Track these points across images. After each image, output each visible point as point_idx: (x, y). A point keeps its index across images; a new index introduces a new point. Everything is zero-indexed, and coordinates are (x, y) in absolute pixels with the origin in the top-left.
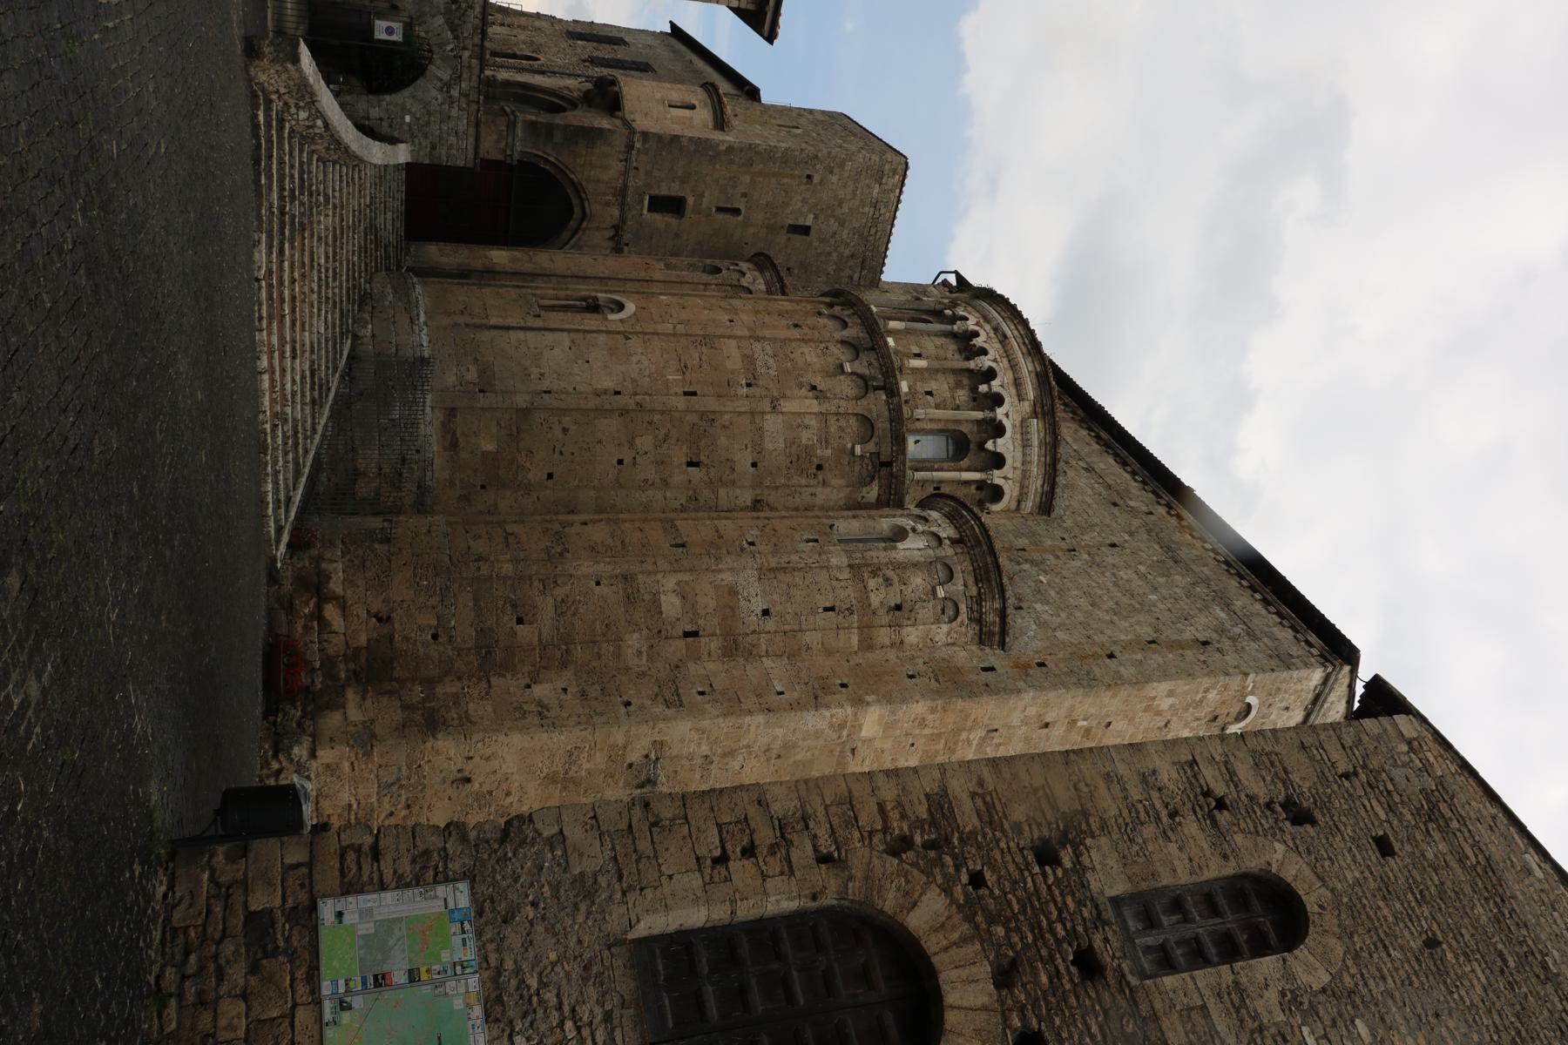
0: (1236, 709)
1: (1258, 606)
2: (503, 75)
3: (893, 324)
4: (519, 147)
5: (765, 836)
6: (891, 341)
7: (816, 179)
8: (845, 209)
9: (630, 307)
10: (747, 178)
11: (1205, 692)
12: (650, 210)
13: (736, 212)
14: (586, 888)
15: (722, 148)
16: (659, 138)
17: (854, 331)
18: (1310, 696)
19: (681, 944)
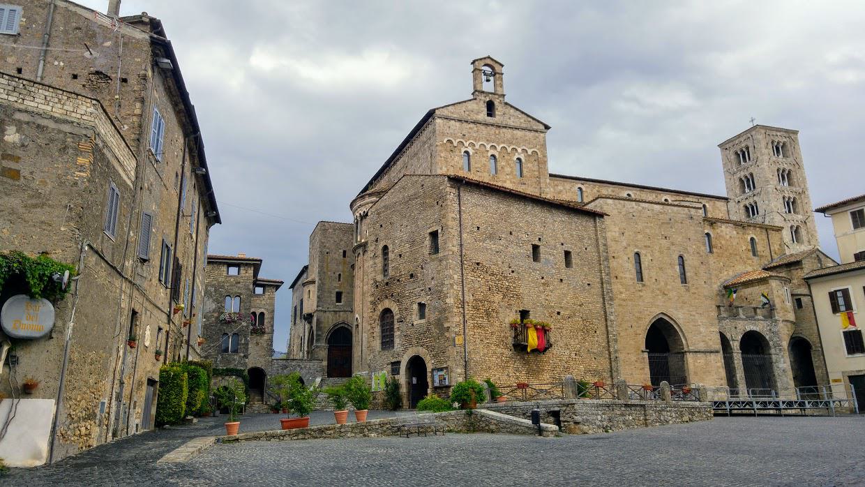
0: (449, 144)
1: (426, 132)
2: (306, 349)
3: (359, 240)
4: (324, 345)
5: (372, 331)
6: (363, 241)
7: (328, 250)
8: (336, 240)
9: (357, 316)
10: (329, 273)
11: (441, 157)
12: (340, 302)
13: (340, 275)
14: (374, 356)
15: (320, 282)
16: (318, 302)
17: (360, 251)
18: (445, 120)
19: (383, 343)
